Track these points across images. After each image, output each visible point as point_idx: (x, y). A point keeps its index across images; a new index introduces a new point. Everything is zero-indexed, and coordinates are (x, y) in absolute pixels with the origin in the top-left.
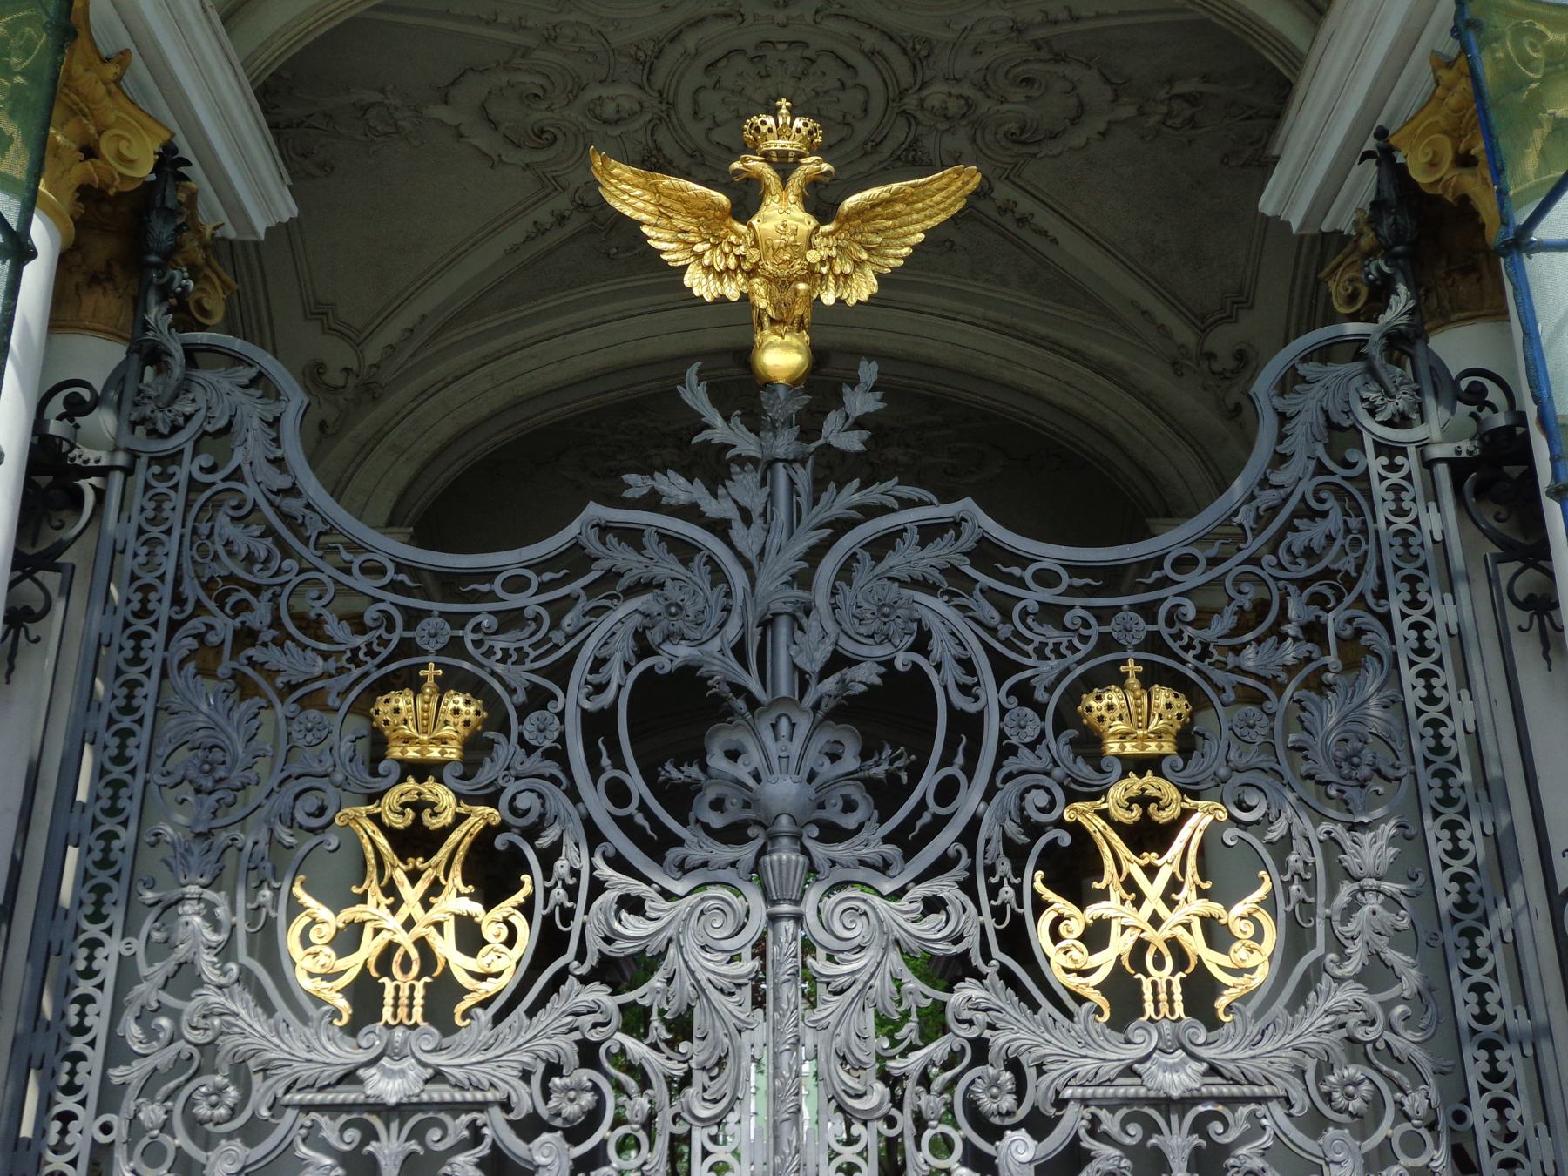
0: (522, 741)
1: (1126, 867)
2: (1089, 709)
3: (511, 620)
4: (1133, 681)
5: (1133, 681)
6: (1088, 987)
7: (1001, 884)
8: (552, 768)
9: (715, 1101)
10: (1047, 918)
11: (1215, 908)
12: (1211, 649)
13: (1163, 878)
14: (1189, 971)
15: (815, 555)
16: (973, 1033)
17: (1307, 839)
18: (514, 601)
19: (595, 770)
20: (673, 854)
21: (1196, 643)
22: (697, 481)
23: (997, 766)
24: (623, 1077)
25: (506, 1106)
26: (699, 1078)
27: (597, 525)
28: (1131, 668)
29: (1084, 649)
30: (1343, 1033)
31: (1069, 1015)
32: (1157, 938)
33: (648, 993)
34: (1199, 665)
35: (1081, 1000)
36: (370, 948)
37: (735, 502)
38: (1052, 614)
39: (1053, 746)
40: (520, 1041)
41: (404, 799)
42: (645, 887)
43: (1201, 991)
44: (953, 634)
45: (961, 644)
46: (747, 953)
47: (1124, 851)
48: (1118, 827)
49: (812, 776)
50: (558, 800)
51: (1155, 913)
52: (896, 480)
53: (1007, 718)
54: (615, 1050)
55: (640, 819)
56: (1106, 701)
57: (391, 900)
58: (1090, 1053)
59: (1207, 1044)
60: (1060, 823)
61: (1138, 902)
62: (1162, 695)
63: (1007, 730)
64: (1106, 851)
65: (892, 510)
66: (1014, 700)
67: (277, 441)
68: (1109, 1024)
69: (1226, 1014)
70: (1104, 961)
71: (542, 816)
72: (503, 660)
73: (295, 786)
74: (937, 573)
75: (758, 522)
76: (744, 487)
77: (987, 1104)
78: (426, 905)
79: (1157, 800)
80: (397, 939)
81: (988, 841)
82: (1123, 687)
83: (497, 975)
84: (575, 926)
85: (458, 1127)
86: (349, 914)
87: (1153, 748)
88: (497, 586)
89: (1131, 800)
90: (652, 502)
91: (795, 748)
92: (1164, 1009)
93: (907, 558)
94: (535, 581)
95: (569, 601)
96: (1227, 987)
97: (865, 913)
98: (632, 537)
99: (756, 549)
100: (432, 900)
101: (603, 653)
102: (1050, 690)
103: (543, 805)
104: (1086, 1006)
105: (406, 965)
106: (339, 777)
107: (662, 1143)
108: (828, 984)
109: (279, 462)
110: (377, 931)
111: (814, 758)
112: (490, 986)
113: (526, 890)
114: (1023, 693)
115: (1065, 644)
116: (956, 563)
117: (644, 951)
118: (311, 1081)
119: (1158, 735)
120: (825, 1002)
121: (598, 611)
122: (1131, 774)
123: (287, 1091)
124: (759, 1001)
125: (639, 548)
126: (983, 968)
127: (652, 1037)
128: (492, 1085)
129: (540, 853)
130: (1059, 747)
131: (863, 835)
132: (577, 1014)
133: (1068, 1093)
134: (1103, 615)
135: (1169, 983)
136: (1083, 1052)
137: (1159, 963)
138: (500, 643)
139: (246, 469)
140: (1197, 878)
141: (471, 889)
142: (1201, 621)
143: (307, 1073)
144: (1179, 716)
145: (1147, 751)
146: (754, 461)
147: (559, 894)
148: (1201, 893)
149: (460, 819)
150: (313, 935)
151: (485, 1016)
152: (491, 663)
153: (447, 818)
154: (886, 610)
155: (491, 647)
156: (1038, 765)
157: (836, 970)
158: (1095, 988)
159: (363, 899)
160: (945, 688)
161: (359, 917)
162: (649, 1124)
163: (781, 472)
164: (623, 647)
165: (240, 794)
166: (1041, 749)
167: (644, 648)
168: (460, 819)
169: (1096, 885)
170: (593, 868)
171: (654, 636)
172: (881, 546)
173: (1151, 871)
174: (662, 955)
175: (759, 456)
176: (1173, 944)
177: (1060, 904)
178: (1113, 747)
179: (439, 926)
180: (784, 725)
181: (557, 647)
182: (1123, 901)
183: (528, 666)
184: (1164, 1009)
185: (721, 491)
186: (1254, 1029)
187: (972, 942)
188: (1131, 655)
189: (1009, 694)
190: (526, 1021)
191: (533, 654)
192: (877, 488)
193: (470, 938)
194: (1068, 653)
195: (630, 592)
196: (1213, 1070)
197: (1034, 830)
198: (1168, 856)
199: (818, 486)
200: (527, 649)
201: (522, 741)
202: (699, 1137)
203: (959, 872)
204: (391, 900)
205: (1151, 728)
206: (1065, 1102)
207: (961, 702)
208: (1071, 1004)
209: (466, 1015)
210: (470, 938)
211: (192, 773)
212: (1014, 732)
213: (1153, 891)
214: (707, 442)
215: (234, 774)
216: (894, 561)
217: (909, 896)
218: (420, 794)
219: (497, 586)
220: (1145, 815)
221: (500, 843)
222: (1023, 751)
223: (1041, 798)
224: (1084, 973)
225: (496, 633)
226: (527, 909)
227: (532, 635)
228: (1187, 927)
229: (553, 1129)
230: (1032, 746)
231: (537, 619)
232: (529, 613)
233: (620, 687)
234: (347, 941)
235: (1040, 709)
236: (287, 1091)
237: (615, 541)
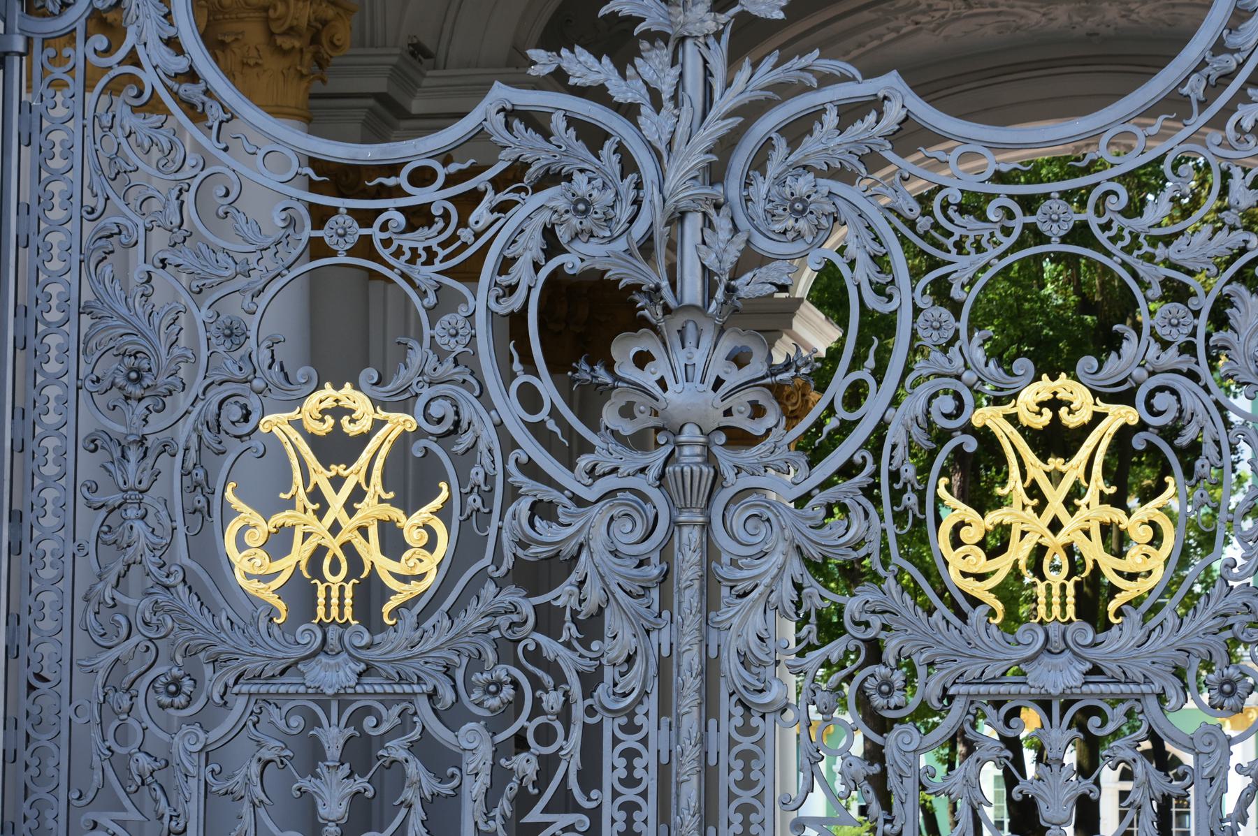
0: (433, 344)
3: (418, 217)
6: (979, 589)
7: (904, 490)
8: (462, 373)
9: (625, 695)
13: (1066, 485)
15: (726, 146)
16: (870, 634)
17: (1217, 443)
18: (420, 196)
19: (508, 377)
20: (584, 461)
21: (1125, 233)
22: (605, 60)
23: (907, 370)
24: (539, 673)
25: (432, 696)
26: (608, 673)
27: (503, 109)
29: (1008, 242)
30: (1228, 634)
31: (963, 616)
33: (563, 595)
35: (975, 602)
36: (301, 552)
37: (645, 83)
38: (973, 206)
40: (443, 639)
41: (323, 406)
42: (556, 493)
43: (1092, 598)
44: (869, 227)
45: (876, 238)
46: (655, 558)
48: (1025, 431)
49: (719, 382)
50: (471, 409)
52: (817, 52)
53: (921, 318)
54: (532, 648)
55: (551, 425)
57: (317, 506)
60: (968, 429)
61: (1039, 510)
63: (920, 333)
65: (810, 89)
67: (168, 16)
68: (998, 626)
70: (1003, 565)
71: (457, 424)
72: (412, 261)
73: (215, 395)
74: (855, 160)
75: (669, 105)
76: (653, 65)
77: (878, 701)
78: (350, 509)
79: (1068, 404)
80: (324, 543)
81: (894, 447)
83: (421, 577)
84: (492, 531)
85: (391, 717)
86: (279, 519)
88: (402, 180)
89: (1041, 404)
90: (559, 80)
91: (699, 357)
92: (1056, 610)
93: (825, 141)
94: (442, 173)
95: (475, 197)
97: (768, 520)
98: (537, 122)
99: (666, 137)
100: (356, 505)
101: (509, 254)
103: (457, 413)
104: (980, 608)
105: (335, 569)
106: (258, 384)
107: (576, 734)
108: (732, 588)
109: (173, 43)
110: (306, 536)
111: (719, 366)
112: (416, 588)
113: (444, 495)
114: (941, 291)
115: (987, 236)
116: (876, 148)
117: (558, 554)
118: (257, 673)
120: (729, 605)
121: (504, 207)
122: (1045, 376)
123: (236, 683)
124: (665, 603)
125: (547, 135)
126: (881, 571)
127: (565, 636)
128: (419, 678)
129: (452, 456)
131: (771, 439)
132: (495, 615)
133: (951, 691)
134: (1029, 204)
138: (408, 242)
139: (140, 51)
141: (391, 495)
142: (1134, 209)
143: (254, 666)
146: (665, 37)
147: (474, 501)
148: (1104, 499)
149: (378, 425)
150: (248, 540)
151: (410, 617)
152: (400, 264)
153: (364, 425)
154: (799, 206)
155: (400, 247)
156: (948, 369)
157: (739, 574)
158: (990, 591)
159: (290, 504)
160: (858, 286)
161: (289, 522)
162: (565, 715)
163: (691, 54)
164: (532, 245)
165: (167, 400)
166: (954, 351)
167: (552, 246)
168: (378, 425)
170: (506, 474)
171: (563, 234)
172: (797, 131)
174: (576, 558)
175: (670, 32)
179: (363, 531)
180: (690, 326)
181: (465, 246)
182: (1024, 507)
183: (438, 266)
184: (1056, 610)
185: (630, 71)
186: (1140, 634)
187: (874, 547)
190: (446, 623)
191: (442, 253)
192: (798, 63)
193: (393, 543)
194: (989, 247)
195: (538, 187)
196: (1096, 670)
199: (733, 60)
200: (435, 248)
201: (433, 344)
202: (610, 727)
203: (862, 478)
204: (317, 506)
206: (951, 699)
207: (873, 301)
208: (965, 606)
209: (395, 613)
210: (393, 543)
211: (120, 381)
213: (1056, 497)
214: (614, 14)
215: (161, 380)
216: (811, 147)
217: (811, 503)
218: (337, 401)
219: (402, 180)
220: (1056, 419)
221: (417, 451)
222: (937, 355)
224: (981, 577)
225: (403, 232)
226: (444, 513)
227: (440, 233)
229: (477, 719)
230: (944, 350)
231: (446, 216)
232: (436, 211)
233: (530, 288)
234: (279, 543)
235: (956, 308)
236: (236, 683)
237: (522, 127)
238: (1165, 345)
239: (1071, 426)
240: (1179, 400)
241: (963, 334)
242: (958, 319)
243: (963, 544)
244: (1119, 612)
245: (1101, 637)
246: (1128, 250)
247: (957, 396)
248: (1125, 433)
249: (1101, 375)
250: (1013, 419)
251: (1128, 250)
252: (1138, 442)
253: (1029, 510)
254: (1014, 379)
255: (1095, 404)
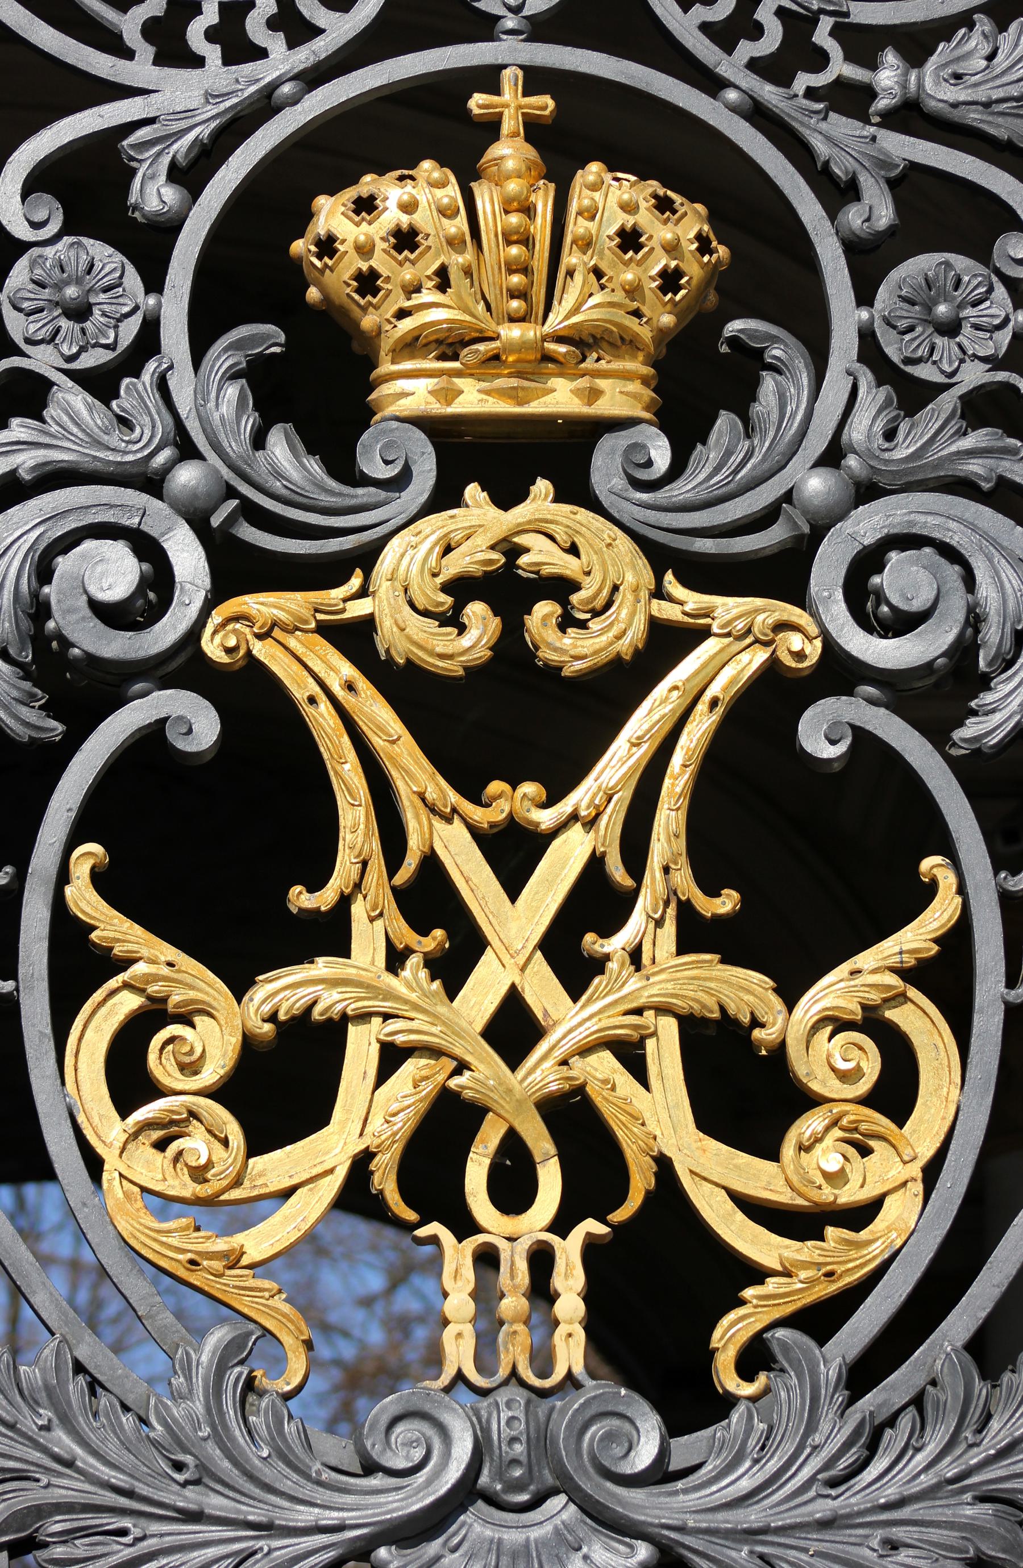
1: (418, 831)
2: (327, 246)
4: (510, 152)
5: (510, 152)
10: (107, 1012)
11: (742, 990)
12: (822, 36)
14: (621, 1215)
28: (511, 103)
32: (513, 1094)
34: (769, 93)
39: (183, 389)
47: (413, 772)
48: (406, 686)
51: (513, 1003)
56: (391, 217)
58: (216, 1503)
59: (660, 1474)
62: (608, 197)
64: (347, 775)
66: (50, 211)
69: (746, 1369)
79: (560, 588)
82: (468, 172)
87: (560, 398)
89: (464, 589)
96: (757, 1274)
102: (191, 175)
119: (584, 342)
122: (473, 492)
130: (214, 397)
135: (541, 1261)
136: (190, 1498)
137: (513, 1189)
140: (684, 880)
144: (670, 280)
145: (536, 407)
148: (695, 934)
166: (136, 392)
169: (301, 899)
173: (514, 854)
176: (573, 1117)
177: (156, 961)
178: (409, 391)
182: (395, 959)
186: (834, 1433)
188: (509, 52)
189: (30, 187)
194: (275, 44)
197: (81, 691)
198: (581, 797)
205: (556, 321)
212: (34, 327)
213: (515, 924)
220: (512, 644)
222: (71, 401)
223: (115, 572)
228: (632, 1056)
230: (101, 384)
235: (148, 247)
238: (911, 395)
239: (572, 668)
240: (969, 581)
241: (175, 337)
242: (154, 283)
243: (155, 1091)
244: (755, 1358)
245: (686, 1448)
246: (775, 70)
247: (147, 548)
248: (772, 700)
249: (681, 490)
250: (354, 639)
251: (775, 70)
252: (820, 734)
253: (414, 968)
254: (363, 494)
255: (659, 593)
